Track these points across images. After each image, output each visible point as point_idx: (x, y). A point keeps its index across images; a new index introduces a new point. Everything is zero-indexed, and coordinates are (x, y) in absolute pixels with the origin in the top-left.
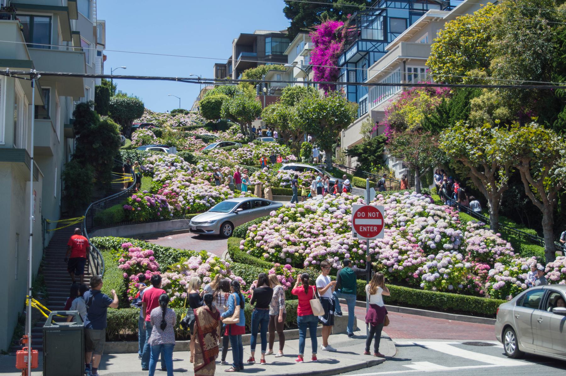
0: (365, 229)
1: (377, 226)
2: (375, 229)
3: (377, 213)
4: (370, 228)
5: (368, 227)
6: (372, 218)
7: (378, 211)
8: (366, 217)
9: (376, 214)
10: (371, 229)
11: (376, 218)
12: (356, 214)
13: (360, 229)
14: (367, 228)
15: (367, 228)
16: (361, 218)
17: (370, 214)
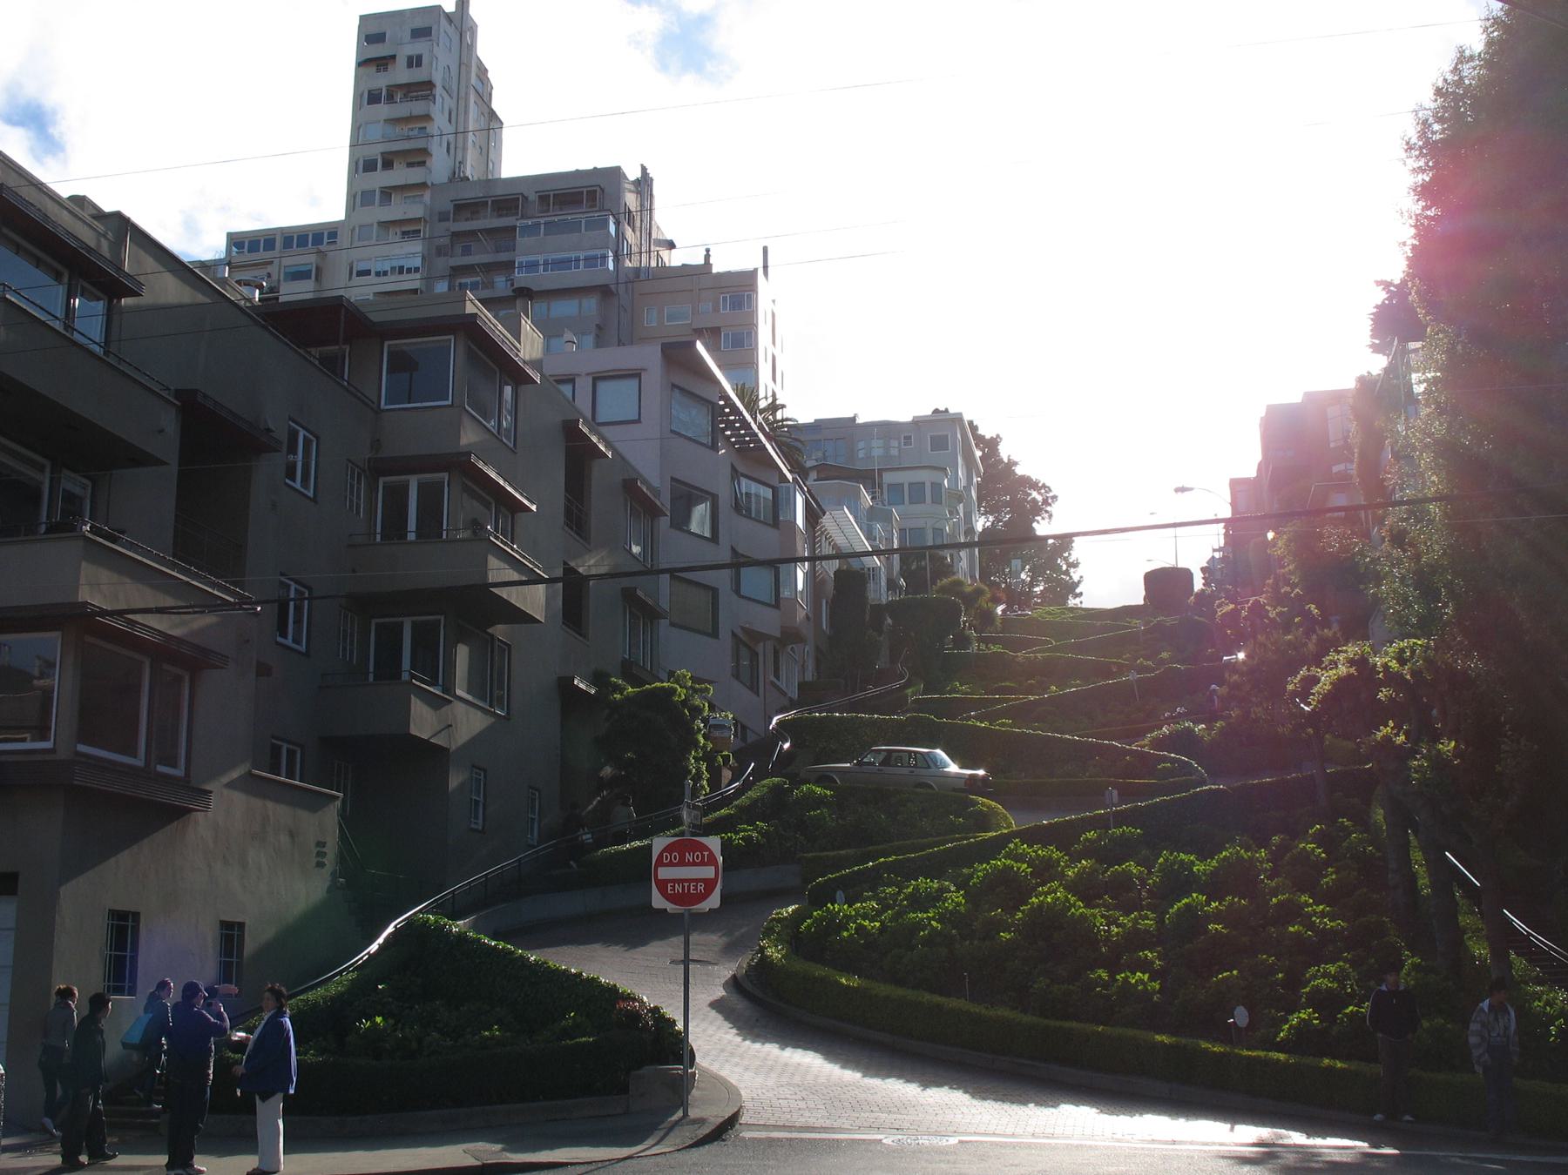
0: (679, 888)
1: (705, 881)
2: (701, 887)
3: (706, 853)
4: (689, 887)
5: (686, 885)
6: (694, 864)
7: (708, 849)
8: (682, 863)
9: (703, 856)
10: (692, 888)
11: (702, 863)
12: (660, 856)
13: (669, 888)
14: (684, 887)
15: (684, 887)
16: (671, 864)
17: (689, 857)
